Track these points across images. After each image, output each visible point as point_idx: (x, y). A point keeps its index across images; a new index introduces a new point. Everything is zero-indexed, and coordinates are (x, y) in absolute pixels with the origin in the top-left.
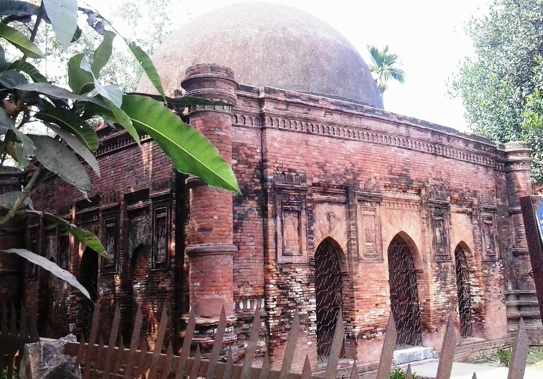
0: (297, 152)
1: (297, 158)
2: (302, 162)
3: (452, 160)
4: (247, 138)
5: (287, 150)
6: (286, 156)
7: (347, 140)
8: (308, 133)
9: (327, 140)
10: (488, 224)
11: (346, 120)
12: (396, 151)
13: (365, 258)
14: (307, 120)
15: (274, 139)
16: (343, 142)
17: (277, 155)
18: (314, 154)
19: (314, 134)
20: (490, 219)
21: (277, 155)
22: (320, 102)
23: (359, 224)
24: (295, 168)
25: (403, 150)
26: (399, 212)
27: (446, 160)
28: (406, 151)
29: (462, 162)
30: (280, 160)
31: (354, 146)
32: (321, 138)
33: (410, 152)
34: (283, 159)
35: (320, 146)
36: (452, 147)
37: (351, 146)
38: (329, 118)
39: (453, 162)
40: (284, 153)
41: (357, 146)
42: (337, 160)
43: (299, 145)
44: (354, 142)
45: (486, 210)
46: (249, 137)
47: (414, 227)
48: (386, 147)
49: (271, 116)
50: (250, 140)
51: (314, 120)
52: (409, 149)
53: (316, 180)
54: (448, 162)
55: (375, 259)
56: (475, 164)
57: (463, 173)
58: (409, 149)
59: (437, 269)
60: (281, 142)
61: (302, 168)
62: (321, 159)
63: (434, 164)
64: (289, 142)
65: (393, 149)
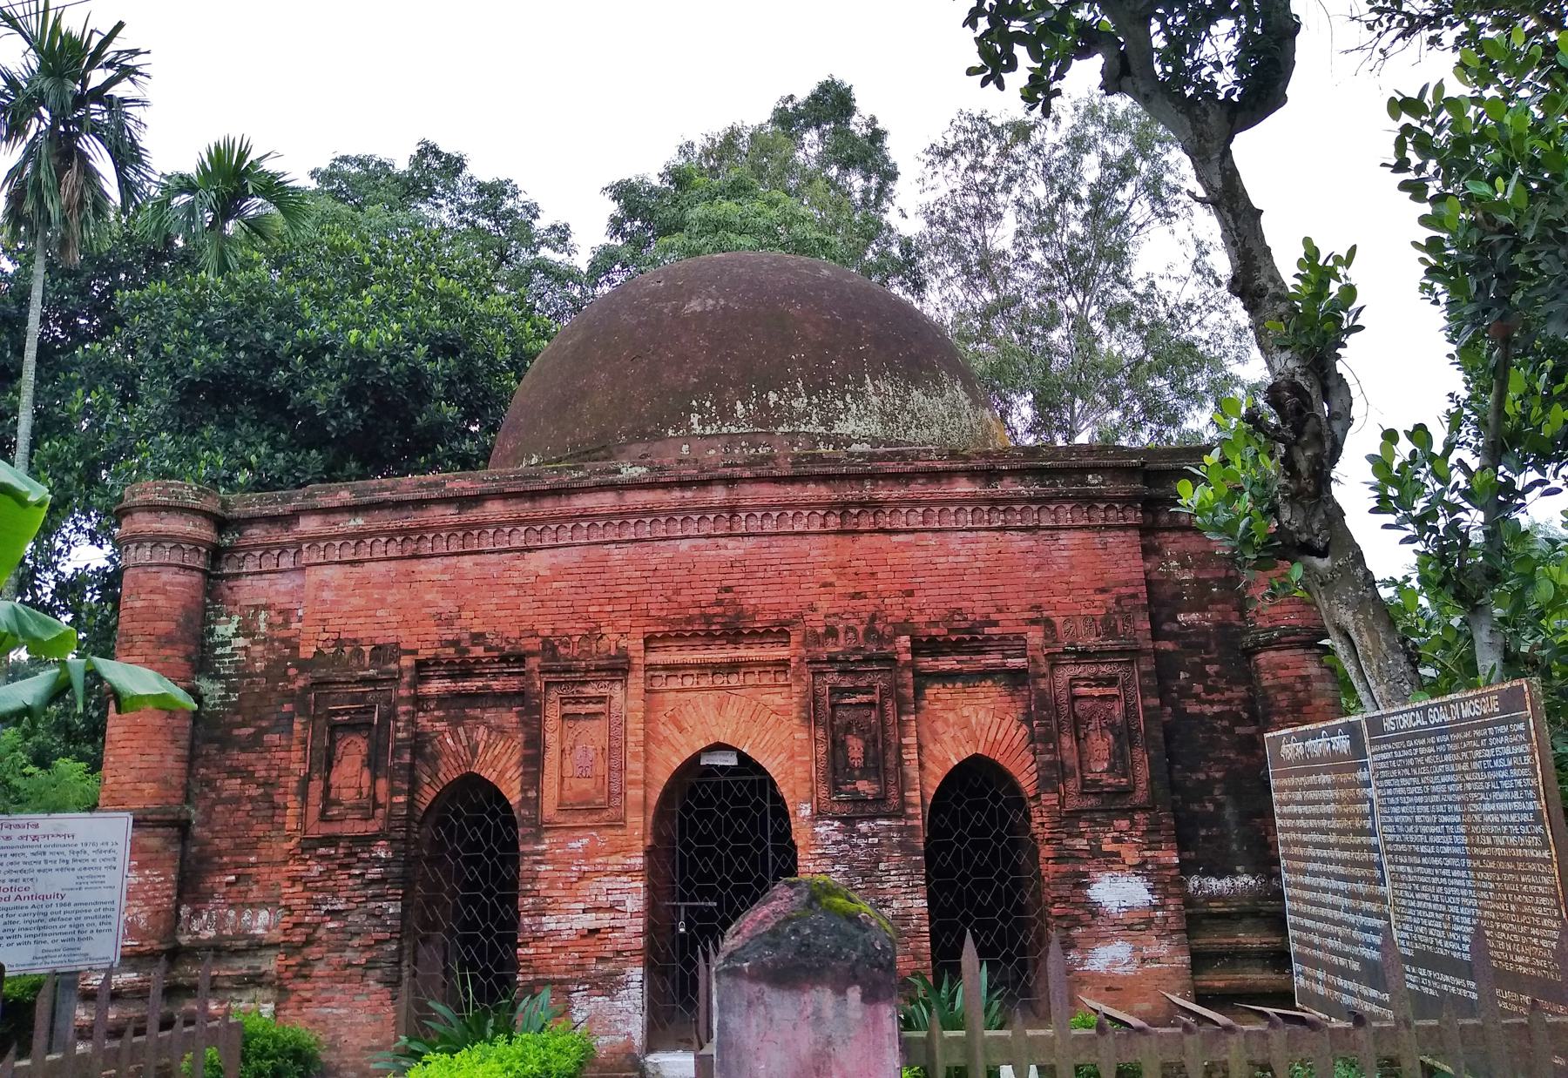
0: (382, 601)
1: (379, 613)
2: (393, 619)
3: (930, 535)
4: (278, 592)
5: (357, 601)
6: (354, 613)
7: (529, 550)
8: (415, 557)
9: (467, 562)
10: (1103, 698)
11: (525, 508)
12: (697, 548)
13: (562, 819)
14: (406, 533)
15: (323, 585)
16: (518, 558)
17: (329, 616)
18: (428, 597)
19: (432, 556)
20: (1111, 681)
21: (329, 616)
22: (448, 486)
23: (551, 738)
24: (373, 634)
25: (722, 541)
26: (712, 697)
27: (895, 538)
28: (731, 543)
29: (968, 534)
30: (335, 622)
31: (554, 560)
32: (454, 560)
33: (750, 542)
34: (343, 621)
35: (446, 577)
36: (917, 502)
37: (539, 562)
38: (472, 515)
39: (932, 540)
40: (346, 608)
41: (560, 559)
42: (495, 601)
43: (388, 586)
44: (551, 552)
45: (1083, 656)
46: (282, 589)
47: (764, 727)
48: (663, 544)
49: (314, 540)
50: (285, 594)
51: (425, 528)
52: (742, 535)
53: (424, 654)
54: (907, 544)
55: (596, 818)
56: (1038, 528)
57: (979, 564)
58: (742, 535)
59: (840, 837)
60: (340, 588)
61: (390, 632)
62: (448, 606)
63: (847, 558)
64: (363, 583)
65: (684, 545)
